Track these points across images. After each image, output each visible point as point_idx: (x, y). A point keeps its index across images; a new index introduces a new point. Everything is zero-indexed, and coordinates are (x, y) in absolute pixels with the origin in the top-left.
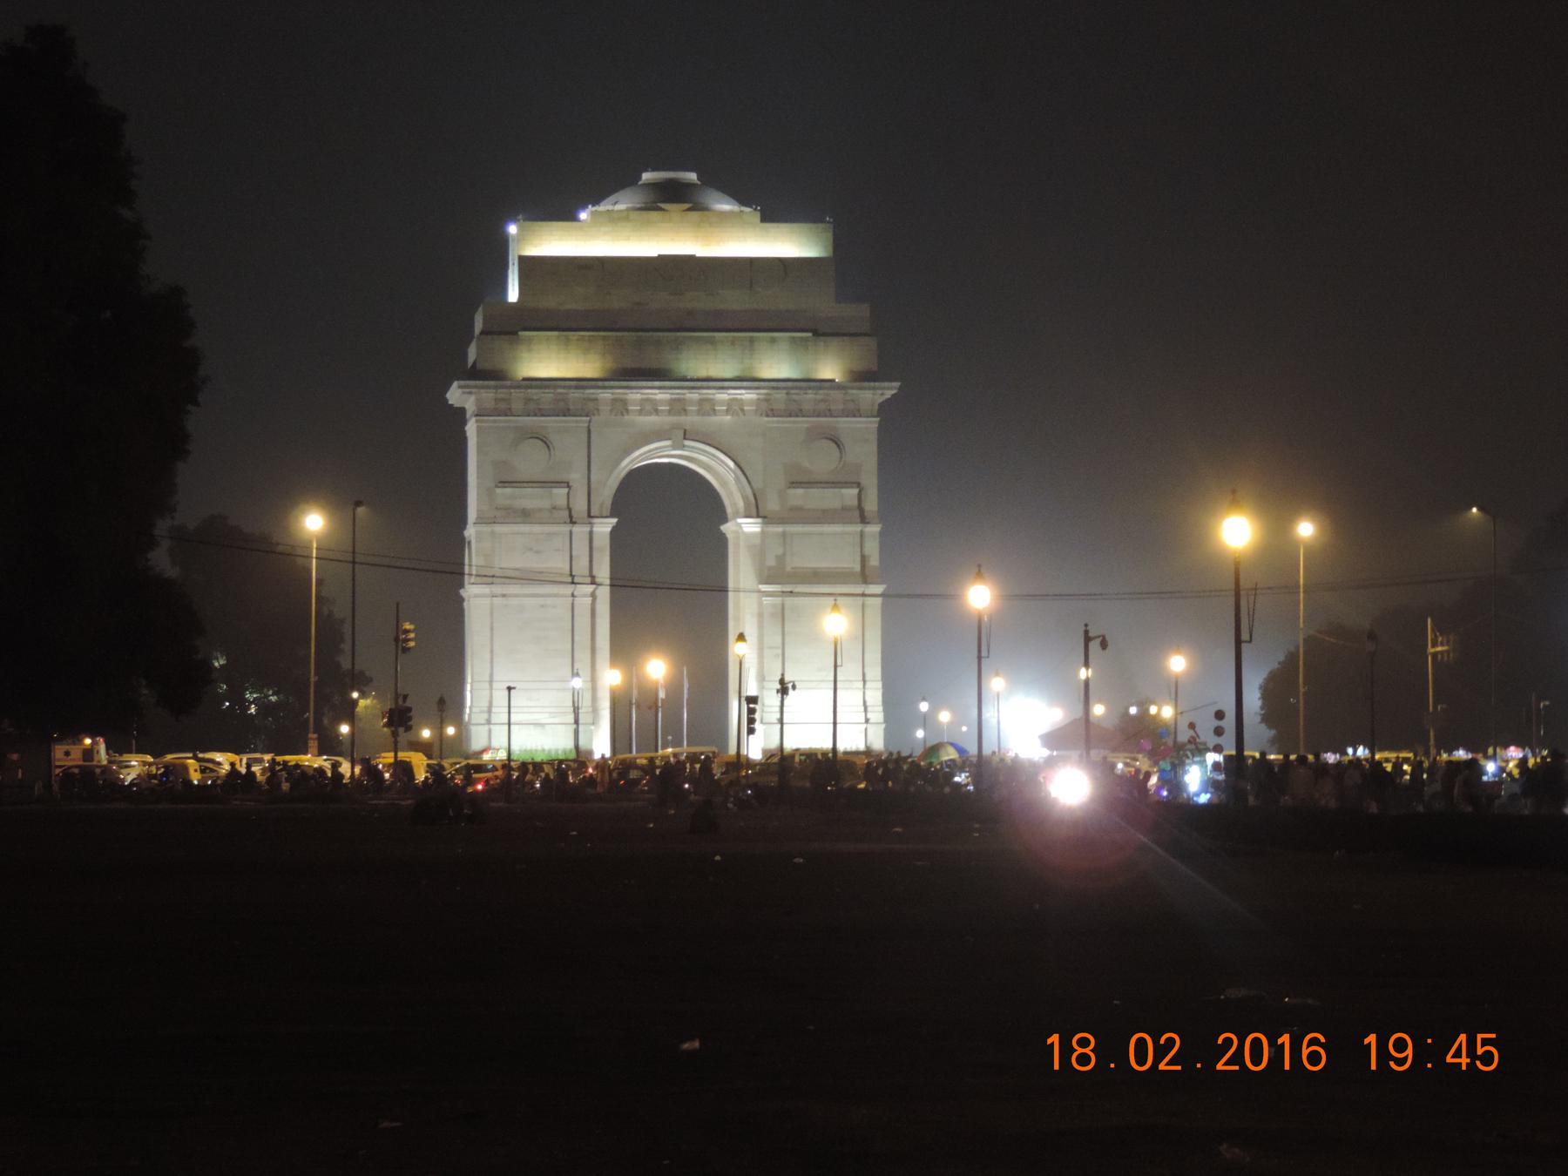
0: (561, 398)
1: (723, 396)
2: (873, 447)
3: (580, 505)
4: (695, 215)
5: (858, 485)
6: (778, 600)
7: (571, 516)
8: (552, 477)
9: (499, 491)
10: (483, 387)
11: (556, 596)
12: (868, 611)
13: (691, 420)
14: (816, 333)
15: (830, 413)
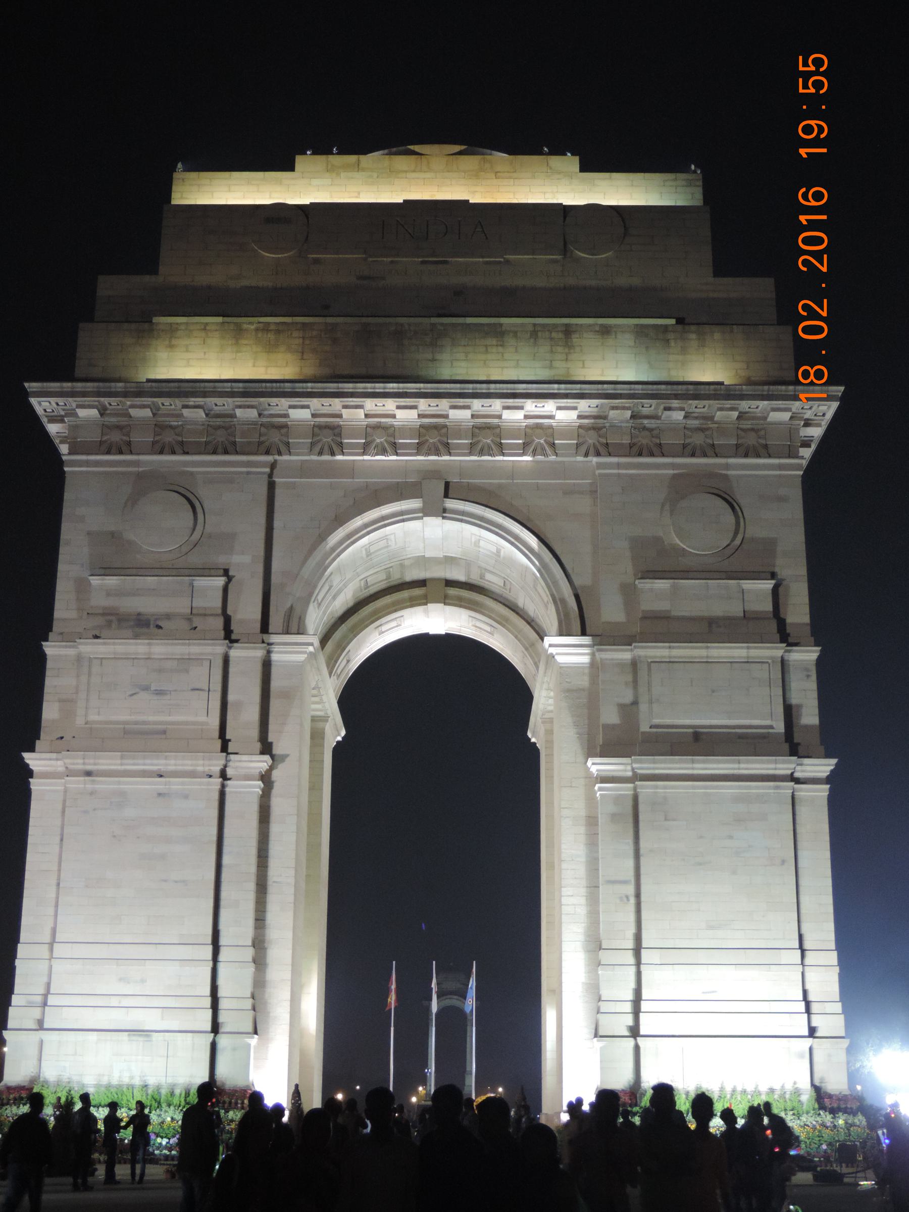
0: (230, 429)
1: (514, 416)
2: (795, 510)
3: (247, 610)
5: (773, 575)
6: (626, 789)
8: (195, 559)
9: (95, 581)
10: (73, 394)
11: (192, 774)
12: (802, 810)
14: (680, 321)
15: (713, 450)
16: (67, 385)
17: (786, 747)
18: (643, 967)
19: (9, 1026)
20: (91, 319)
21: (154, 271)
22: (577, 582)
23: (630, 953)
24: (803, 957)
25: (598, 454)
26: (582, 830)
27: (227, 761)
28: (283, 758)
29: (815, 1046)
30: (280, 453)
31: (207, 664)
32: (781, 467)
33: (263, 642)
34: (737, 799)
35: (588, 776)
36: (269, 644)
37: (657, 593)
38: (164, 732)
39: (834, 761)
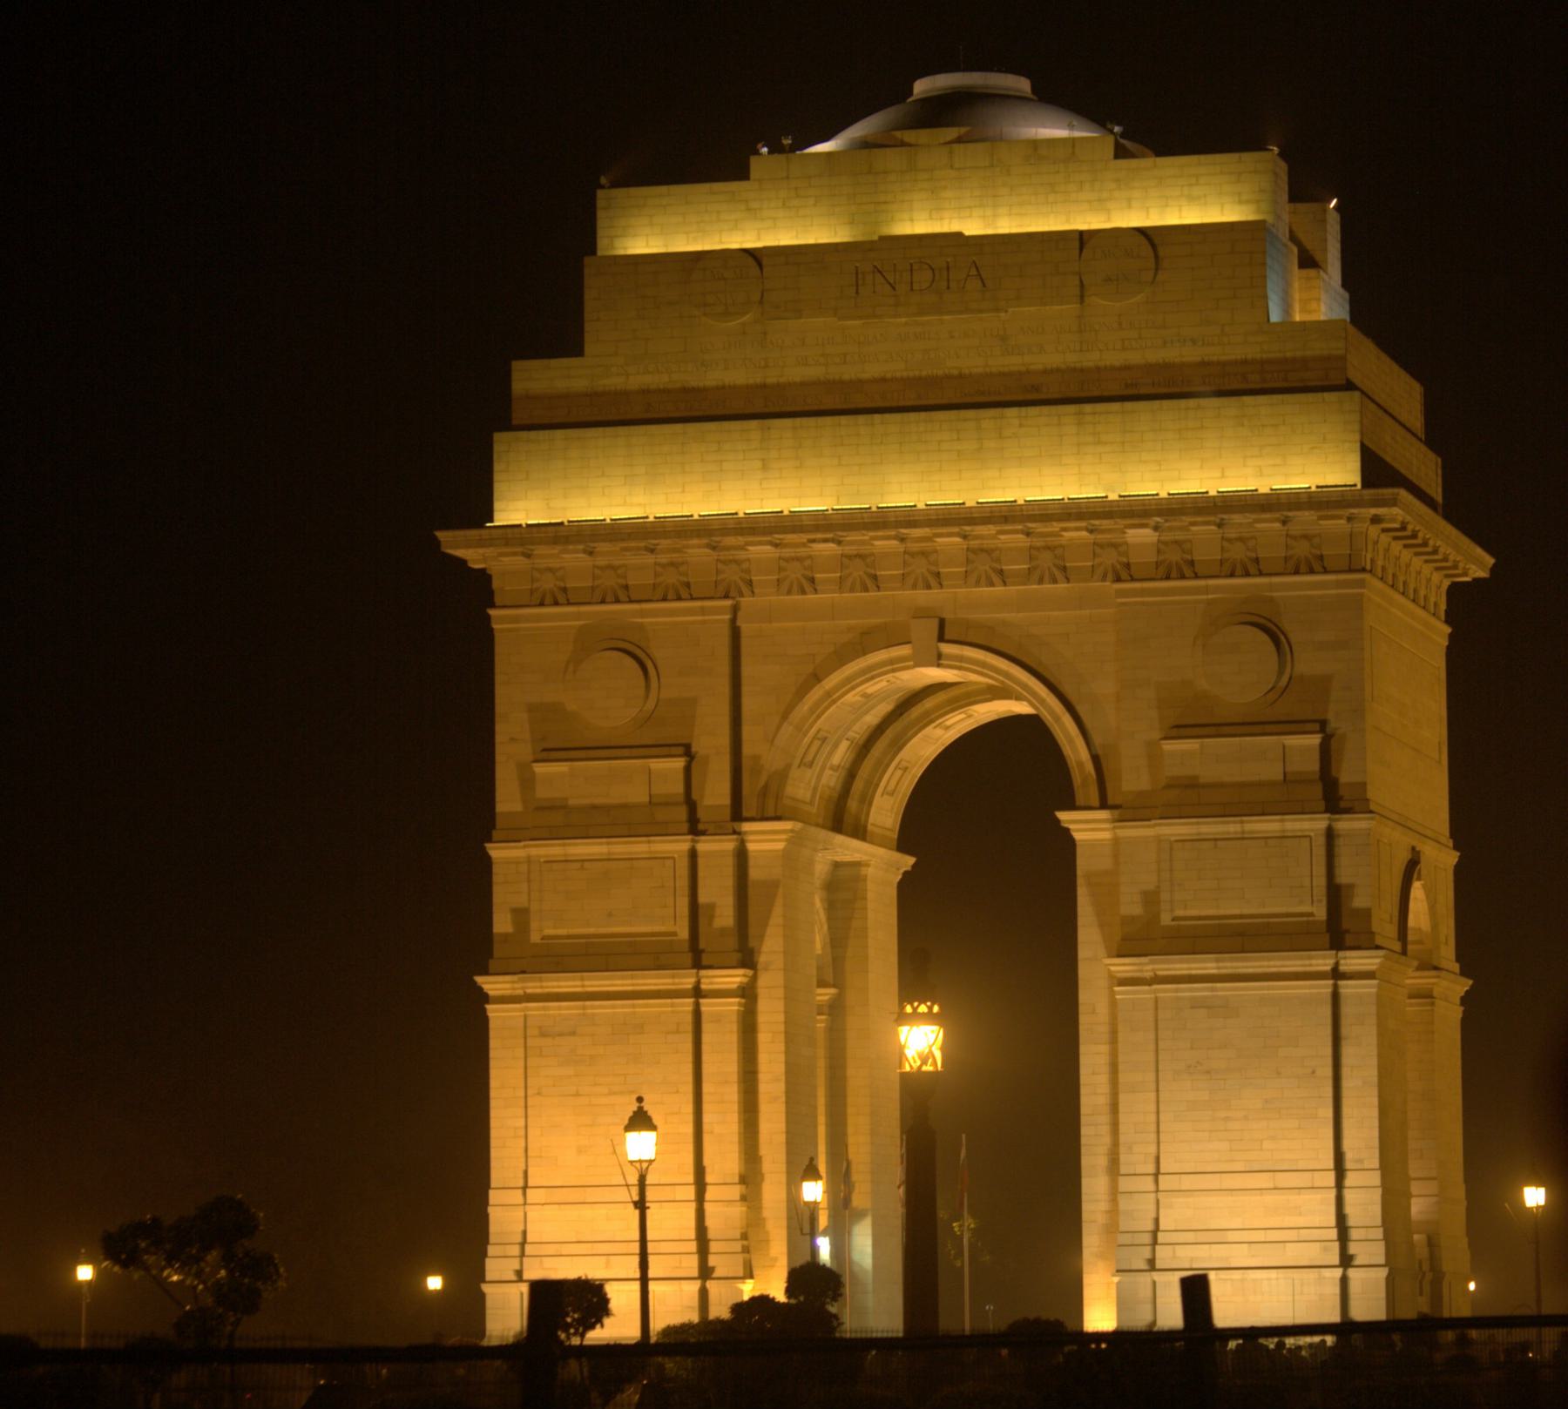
3: (715, 793)
6: (1144, 993)
9: (540, 769)
12: (1347, 1010)
17: (1326, 938)
19: (489, 1277)
20: (508, 427)
22: (1097, 739)
25: (1118, 580)
30: (741, 595)
32: (1339, 584)
33: (735, 832)
35: (1111, 976)
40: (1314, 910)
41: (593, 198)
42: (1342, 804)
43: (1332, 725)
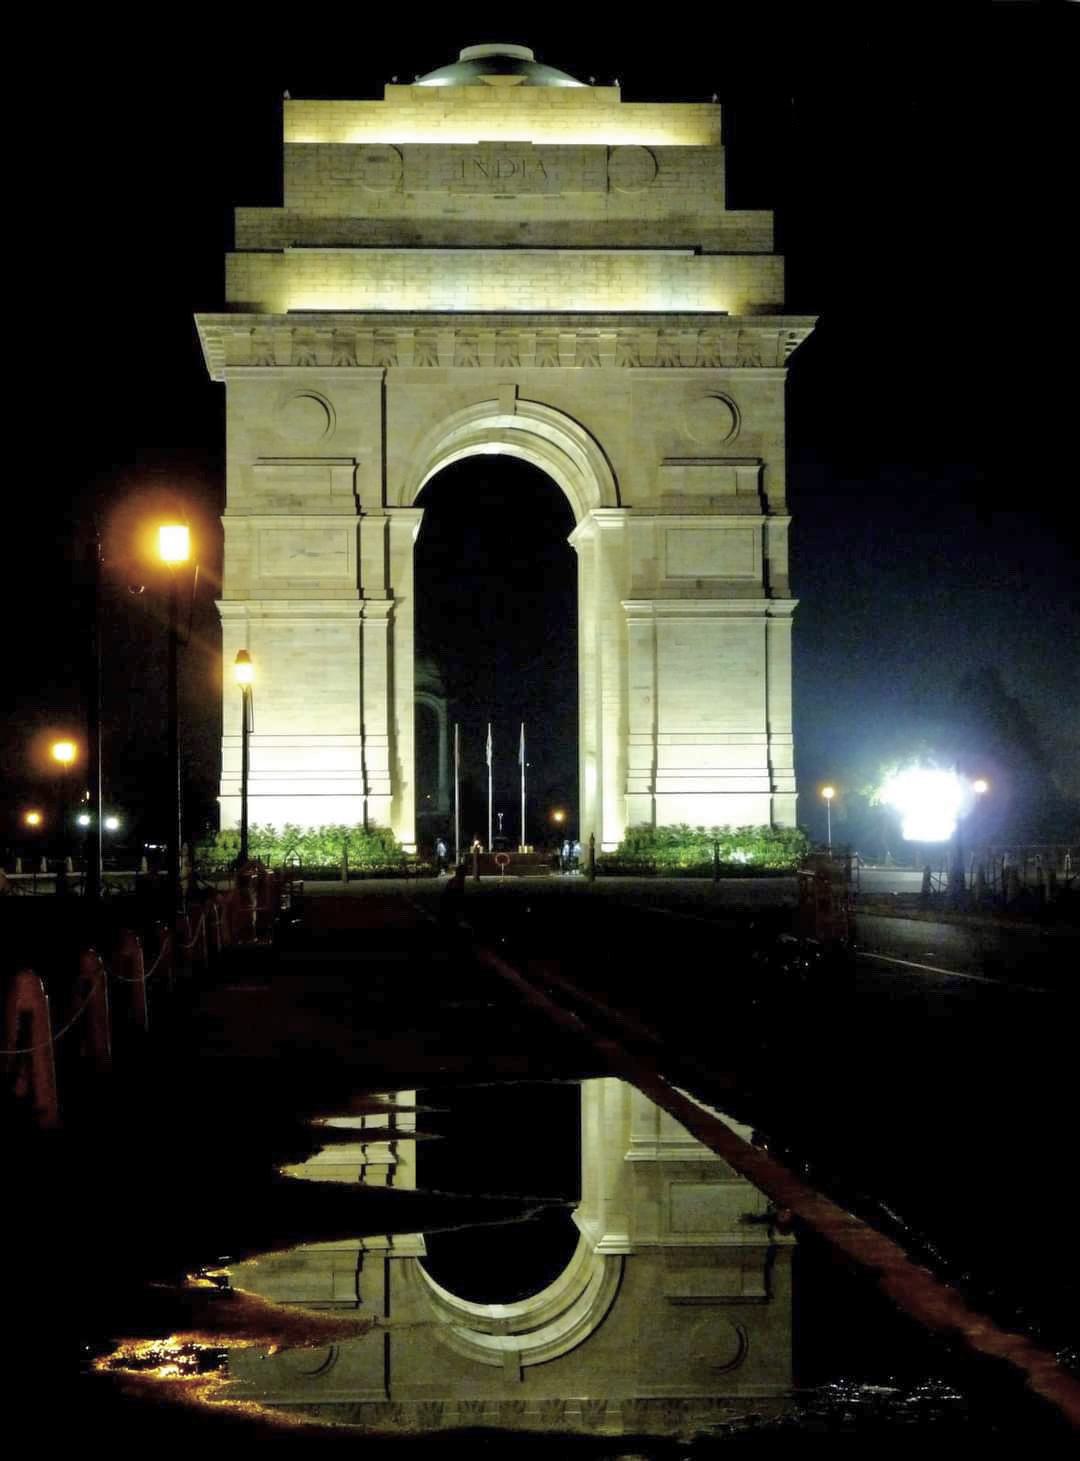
2: (778, 408)
3: (371, 492)
4: (528, 93)
7: (358, 506)
8: (329, 451)
9: (257, 469)
10: (232, 323)
12: (773, 636)
13: (527, 372)
14: (698, 251)
15: (717, 362)
16: (228, 316)
17: (762, 592)
18: (658, 747)
19: (222, 793)
20: (234, 250)
21: (278, 202)
23: (650, 737)
24: (769, 738)
25: (632, 366)
26: (616, 649)
27: (365, 605)
28: (402, 600)
29: (775, 798)
30: (390, 365)
31: (345, 533)
34: (726, 629)
35: (623, 611)
36: (390, 516)
37: (675, 477)
38: (317, 585)
39: (796, 602)
40: (755, 574)
41: (281, 105)
42: (771, 511)
43: (764, 462)
